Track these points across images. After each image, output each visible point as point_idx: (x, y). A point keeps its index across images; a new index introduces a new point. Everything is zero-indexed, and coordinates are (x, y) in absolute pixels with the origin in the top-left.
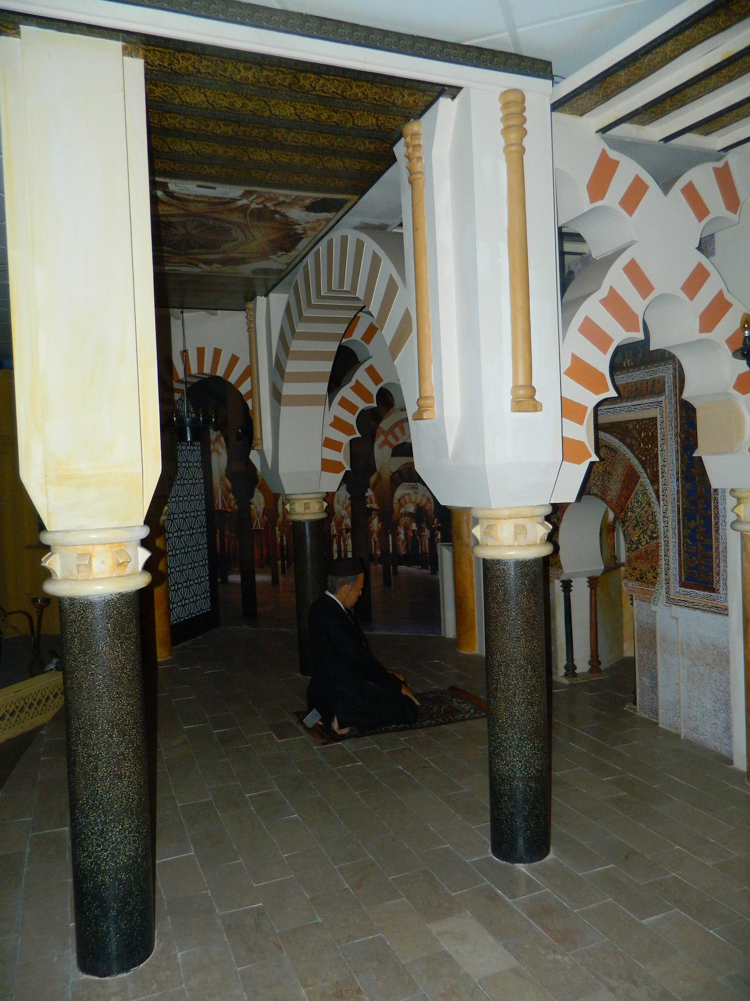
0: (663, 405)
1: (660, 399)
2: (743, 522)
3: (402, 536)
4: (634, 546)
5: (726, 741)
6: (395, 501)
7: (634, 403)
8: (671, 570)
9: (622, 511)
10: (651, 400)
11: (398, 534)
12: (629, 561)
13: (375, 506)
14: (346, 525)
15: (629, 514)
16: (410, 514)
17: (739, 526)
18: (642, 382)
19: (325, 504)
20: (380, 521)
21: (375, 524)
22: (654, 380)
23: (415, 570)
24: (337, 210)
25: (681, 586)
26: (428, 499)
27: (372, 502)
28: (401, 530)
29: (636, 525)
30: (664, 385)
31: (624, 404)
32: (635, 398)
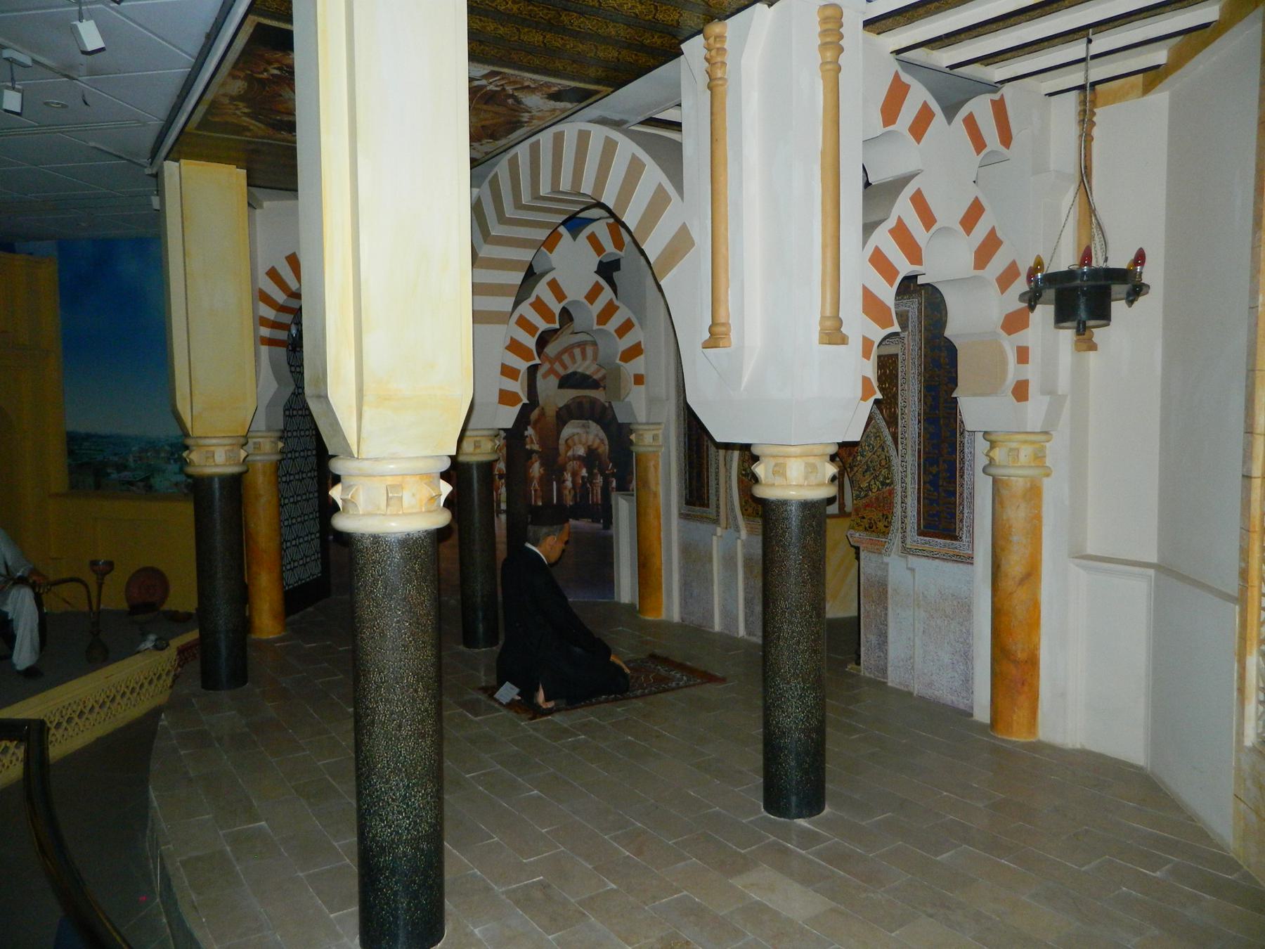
2: (999, 466)
3: (569, 484)
4: (863, 494)
5: (964, 694)
6: (562, 442)
11: (564, 481)
12: (857, 510)
13: (536, 447)
14: (500, 470)
16: (579, 458)
17: (993, 471)
20: (542, 465)
21: (536, 469)
23: (583, 524)
24: (580, 102)
25: (919, 534)
26: (602, 441)
27: (532, 442)
28: (568, 477)
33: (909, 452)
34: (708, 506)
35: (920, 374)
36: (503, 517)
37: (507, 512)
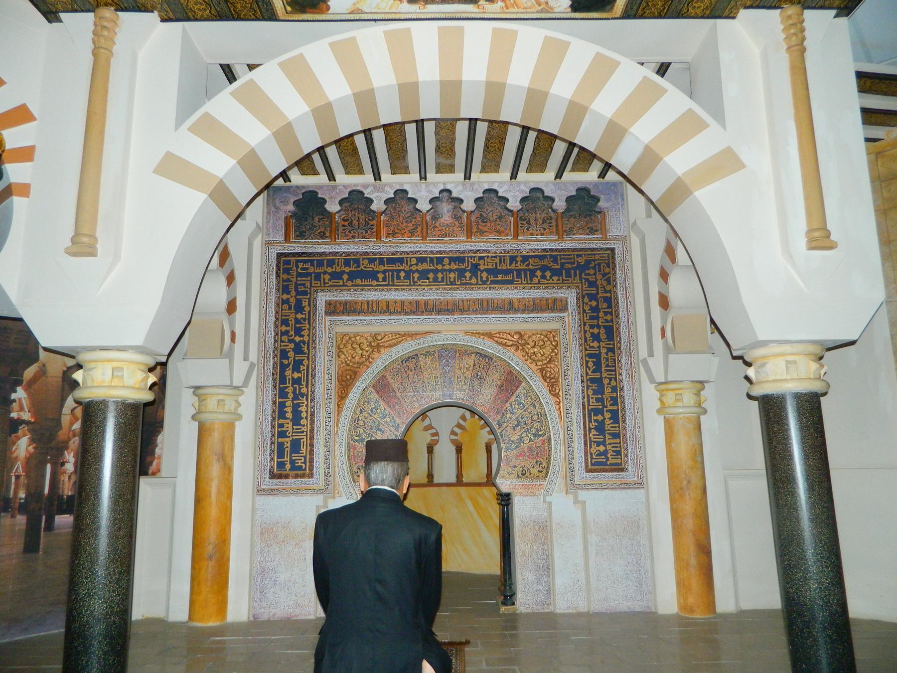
0: (566, 319)
1: (562, 315)
3: (70, 467)
5: (639, 597)
7: (531, 315)
8: (576, 459)
9: (498, 413)
10: (552, 315)
11: (63, 464)
13: (26, 416)
15: (508, 416)
18: (541, 299)
19: (152, 379)
20: (32, 440)
21: (23, 446)
22: (556, 300)
25: (588, 471)
27: (21, 409)
29: (517, 426)
30: (567, 304)
31: (519, 315)
32: (532, 311)
33: (574, 405)
34: (311, 476)
35: (580, 345)
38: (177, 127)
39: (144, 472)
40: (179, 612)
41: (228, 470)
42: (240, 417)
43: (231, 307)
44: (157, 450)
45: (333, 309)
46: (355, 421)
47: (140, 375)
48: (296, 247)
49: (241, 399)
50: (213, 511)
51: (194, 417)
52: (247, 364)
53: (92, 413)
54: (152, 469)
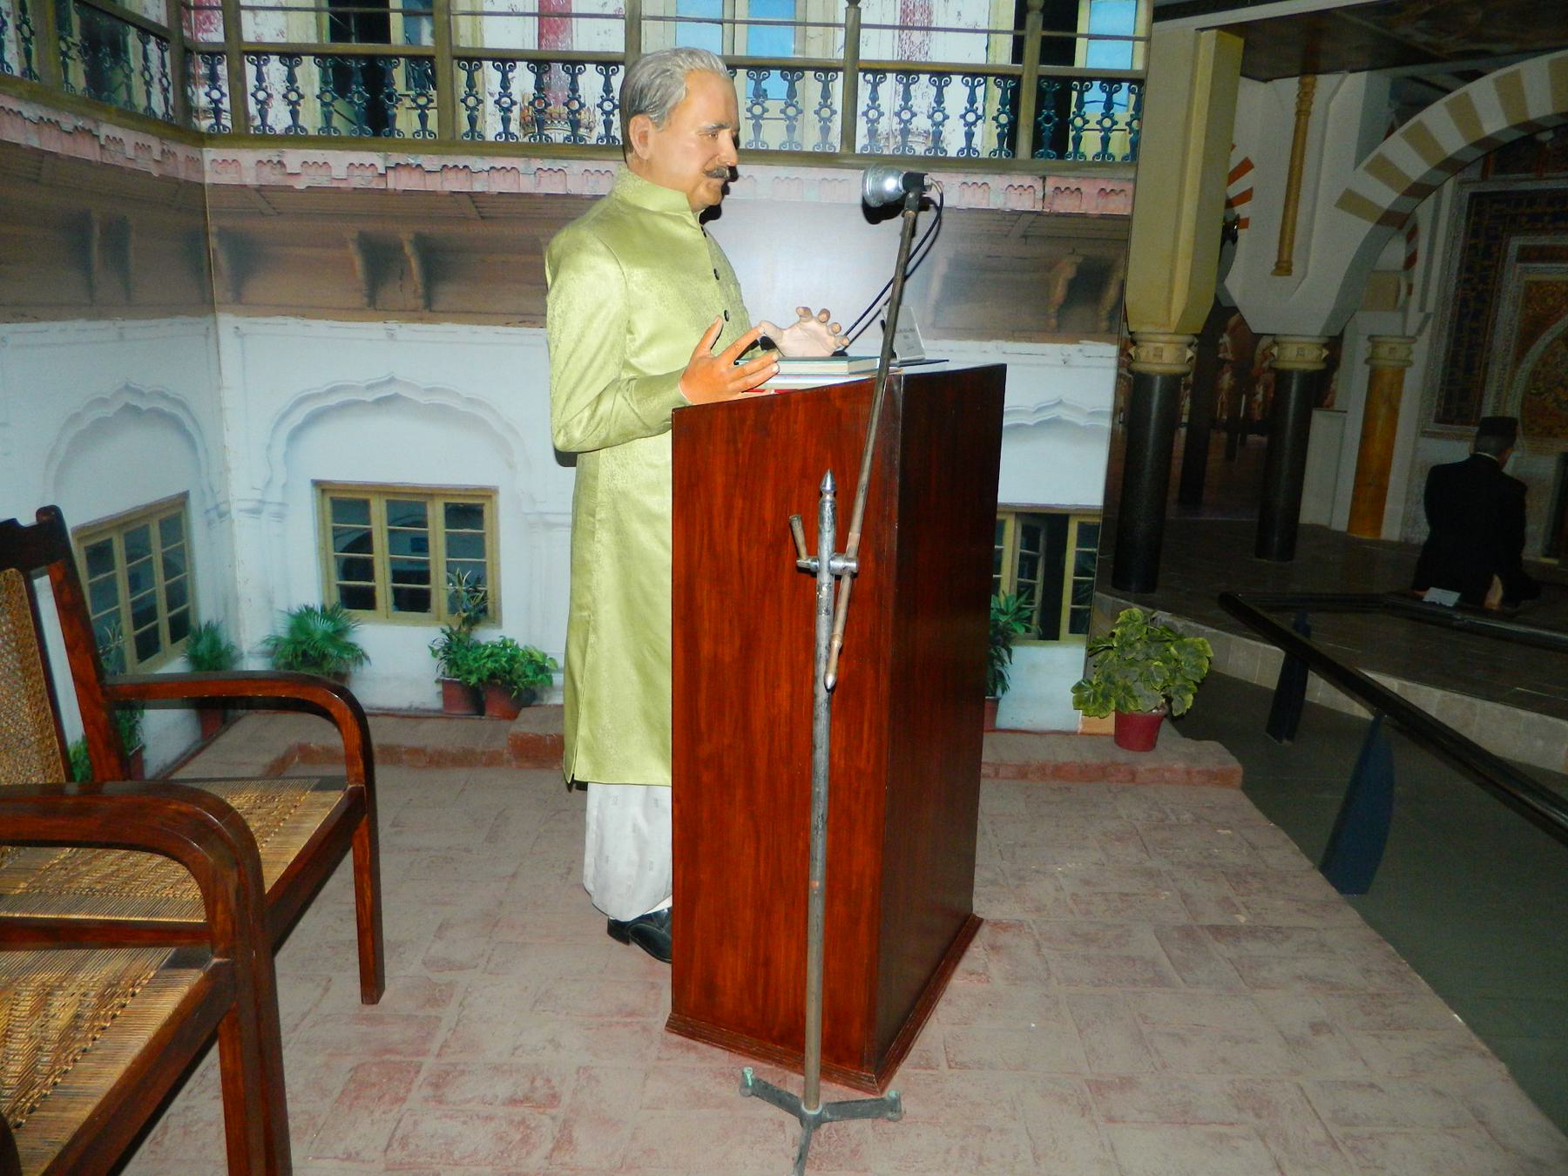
3: (1259, 397)
6: (1258, 352)
13: (1229, 356)
19: (1325, 353)
20: (1233, 376)
21: (1226, 380)
36: (1183, 431)
37: (1189, 425)
38: (1357, 164)
39: (1320, 404)
40: (1340, 522)
41: (1394, 412)
42: (1410, 364)
43: (1411, 261)
44: (1333, 386)
45: (1526, 255)
46: (1535, 375)
47: (1316, 353)
48: (1491, 187)
49: (1414, 347)
50: (1377, 447)
51: (1367, 362)
52: (1422, 315)
53: (1282, 377)
54: (1326, 402)
